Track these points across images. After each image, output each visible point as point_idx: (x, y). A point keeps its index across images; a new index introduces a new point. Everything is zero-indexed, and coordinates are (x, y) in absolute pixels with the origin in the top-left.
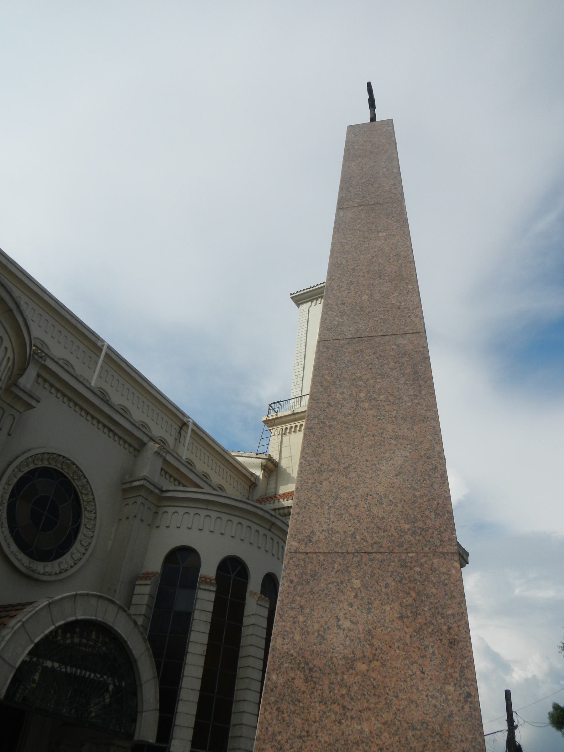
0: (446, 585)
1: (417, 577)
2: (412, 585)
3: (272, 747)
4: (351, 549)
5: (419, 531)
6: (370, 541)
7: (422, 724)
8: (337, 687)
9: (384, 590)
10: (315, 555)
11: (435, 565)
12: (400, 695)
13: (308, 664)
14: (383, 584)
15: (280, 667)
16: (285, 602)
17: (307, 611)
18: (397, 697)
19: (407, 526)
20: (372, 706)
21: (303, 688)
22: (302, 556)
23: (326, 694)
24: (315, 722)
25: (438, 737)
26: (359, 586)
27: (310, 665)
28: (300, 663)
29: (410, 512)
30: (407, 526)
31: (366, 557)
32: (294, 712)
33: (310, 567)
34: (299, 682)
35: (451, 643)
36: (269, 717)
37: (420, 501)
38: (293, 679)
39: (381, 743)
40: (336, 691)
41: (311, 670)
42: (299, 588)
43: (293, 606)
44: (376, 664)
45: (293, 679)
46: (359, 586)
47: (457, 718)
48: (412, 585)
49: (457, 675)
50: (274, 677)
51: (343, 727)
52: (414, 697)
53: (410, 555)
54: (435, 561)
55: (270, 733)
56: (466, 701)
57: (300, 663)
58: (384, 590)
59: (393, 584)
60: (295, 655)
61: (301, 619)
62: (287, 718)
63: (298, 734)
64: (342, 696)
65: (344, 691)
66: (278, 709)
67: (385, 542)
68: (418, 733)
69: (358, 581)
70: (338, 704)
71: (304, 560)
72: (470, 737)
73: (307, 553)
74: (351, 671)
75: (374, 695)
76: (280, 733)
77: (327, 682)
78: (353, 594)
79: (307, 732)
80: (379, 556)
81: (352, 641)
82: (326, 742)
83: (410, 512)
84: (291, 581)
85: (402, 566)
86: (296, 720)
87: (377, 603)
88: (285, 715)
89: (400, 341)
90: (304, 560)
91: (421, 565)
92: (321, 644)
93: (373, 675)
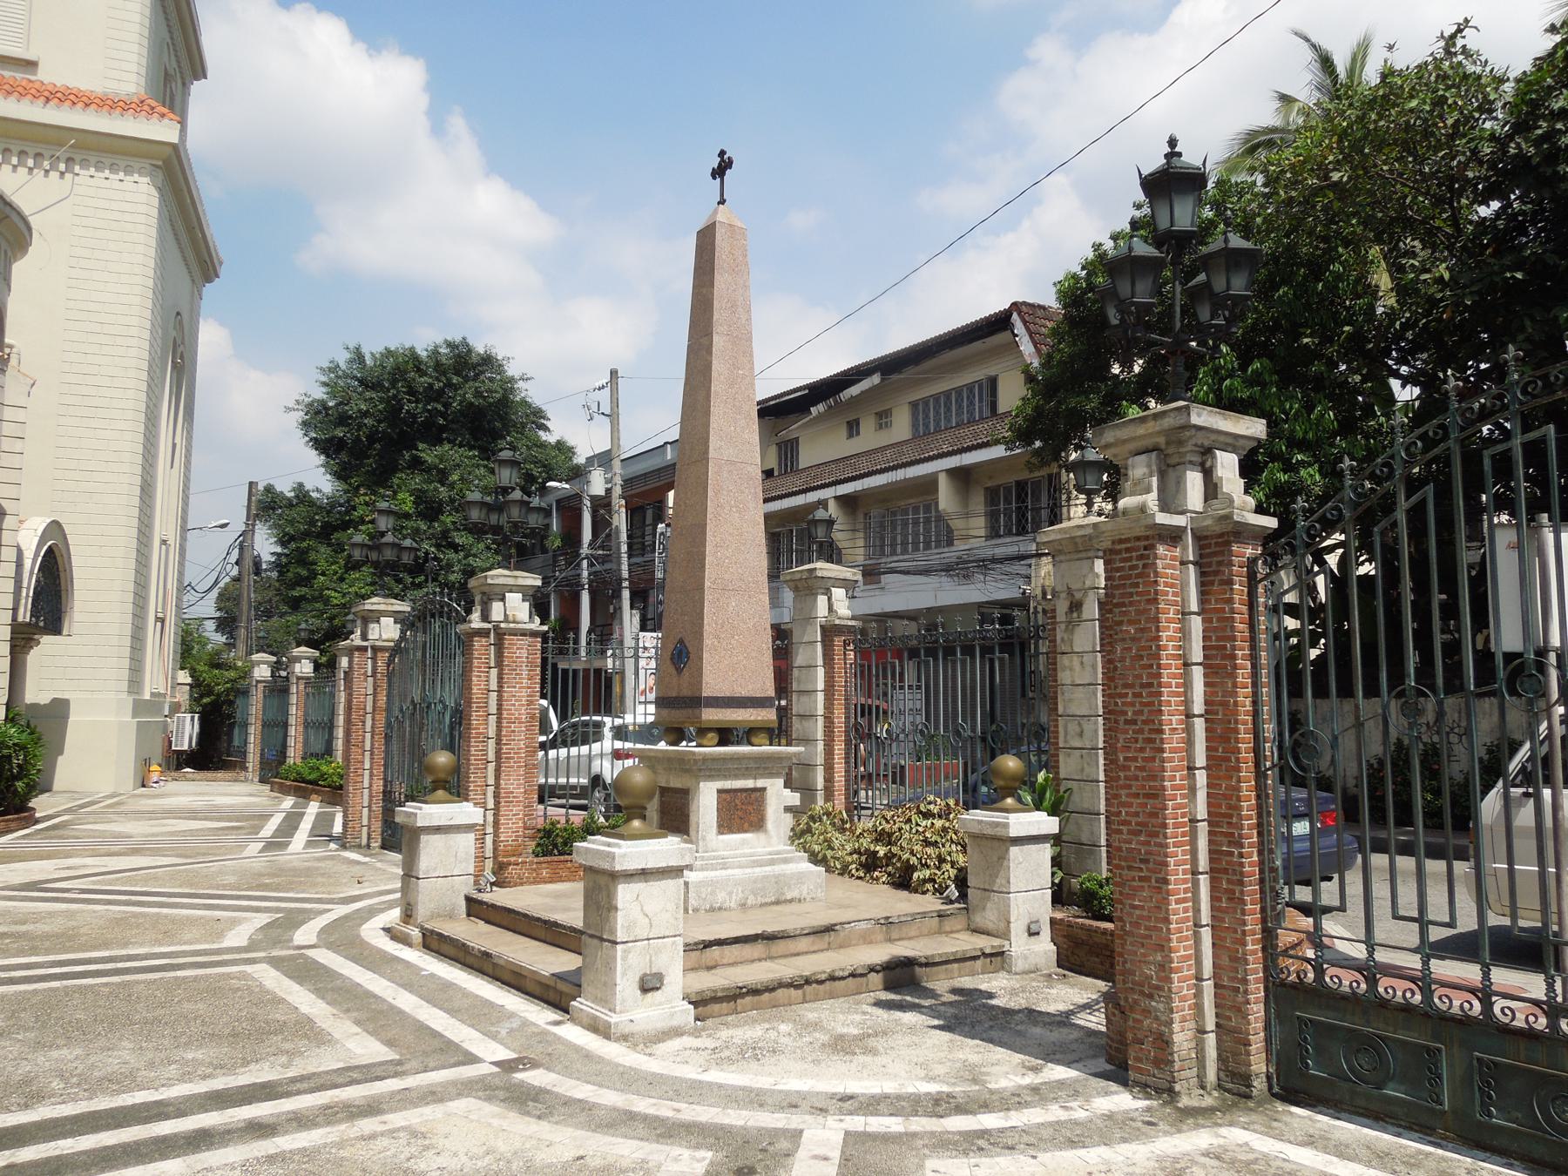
89: (749, 469)
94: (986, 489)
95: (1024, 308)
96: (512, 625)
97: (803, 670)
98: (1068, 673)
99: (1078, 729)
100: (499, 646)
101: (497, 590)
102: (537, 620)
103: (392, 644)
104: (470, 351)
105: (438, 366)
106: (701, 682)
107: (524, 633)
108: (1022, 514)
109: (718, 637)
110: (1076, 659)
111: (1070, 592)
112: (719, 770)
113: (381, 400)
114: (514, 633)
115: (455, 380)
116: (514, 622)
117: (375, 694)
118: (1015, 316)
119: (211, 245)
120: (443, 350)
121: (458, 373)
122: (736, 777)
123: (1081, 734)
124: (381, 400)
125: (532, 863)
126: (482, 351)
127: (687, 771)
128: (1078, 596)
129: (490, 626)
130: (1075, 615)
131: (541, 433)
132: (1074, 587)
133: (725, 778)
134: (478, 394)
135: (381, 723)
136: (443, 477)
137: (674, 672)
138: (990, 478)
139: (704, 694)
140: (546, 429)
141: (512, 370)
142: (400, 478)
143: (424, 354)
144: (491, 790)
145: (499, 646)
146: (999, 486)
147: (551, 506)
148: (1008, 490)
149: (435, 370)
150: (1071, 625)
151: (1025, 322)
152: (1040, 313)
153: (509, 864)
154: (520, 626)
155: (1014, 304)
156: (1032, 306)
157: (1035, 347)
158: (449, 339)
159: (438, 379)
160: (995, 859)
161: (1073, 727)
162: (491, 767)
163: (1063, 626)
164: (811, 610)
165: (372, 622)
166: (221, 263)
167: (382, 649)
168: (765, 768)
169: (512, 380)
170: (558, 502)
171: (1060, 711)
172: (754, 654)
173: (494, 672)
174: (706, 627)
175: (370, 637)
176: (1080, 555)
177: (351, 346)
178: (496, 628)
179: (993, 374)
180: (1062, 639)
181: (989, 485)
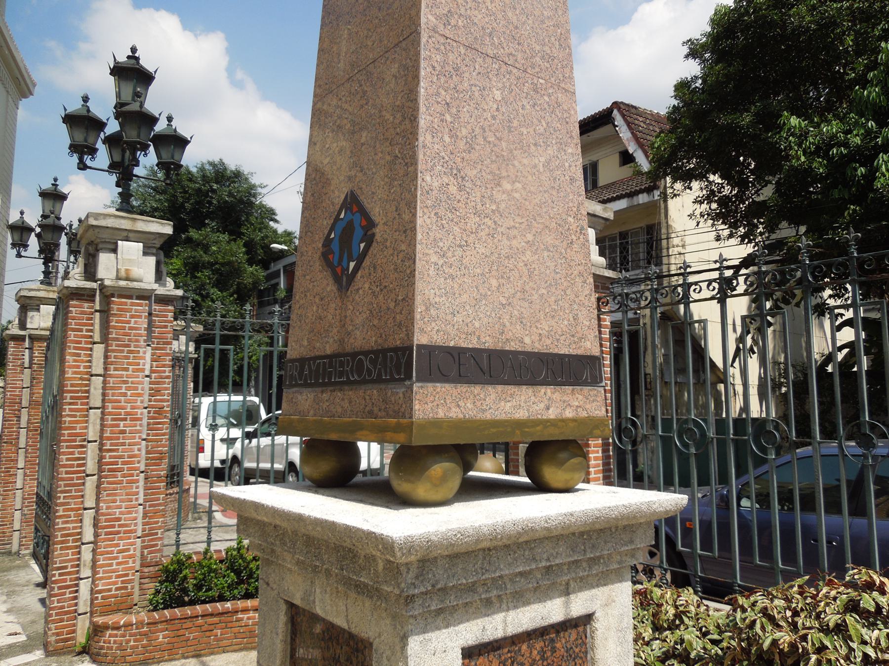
0: (567, 123)
1: (546, 106)
2: (542, 114)
3: (435, 253)
4: (490, 52)
5: (547, 57)
6: (507, 51)
7: (554, 247)
8: (488, 202)
9: (521, 110)
10: (455, 44)
11: (560, 99)
12: (538, 218)
13: (460, 172)
14: (520, 104)
15: (432, 169)
16: (431, 92)
17: (454, 110)
18: (535, 220)
19: (538, 48)
20: (517, 225)
21: (458, 197)
22: (442, 40)
23: (479, 206)
24: (472, 233)
25: (564, 259)
26: (500, 98)
27: (462, 173)
28: (451, 169)
29: (540, 32)
30: (538, 48)
31: (504, 67)
32: (452, 221)
33: (451, 56)
34: (453, 189)
35: (571, 179)
36: (428, 221)
37: (547, 23)
38: (448, 184)
39: (526, 260)
40: (488, 206)
41: (463, 178)
42: (443, 79)
43: (439, 100)
44: (518, 185)
45: (448, 184)
46: (500, 98)
47: (576, 246)
48: (542, 114)
49: (575, 209)
50: (428, 178)
51: (496, 241)
52: (548, 223)
53: (541, 81)
54: (560, 95)
55: (431, 238)
56: (581, 233)
57: (451, 169)
58: (521, 110)
59: (528, 107)
60: (447, 158)
61: (448, 118)
62: (446, 226)
63: (458, 243)
64: (493, 211)
65: (494, 207)
66: (436, 214)
67: (519, 56)
68: (551, 254)
69: (498, 93)
70: (490, 219)
71: (444, 44)
72: (584, 262)
73: (447, 38)
74: (499, 188)
75: (519, 215)
76: (441, 239)
77: (478, 194)
78: (495, 106)
79: (466, 242)
80: (515, 71)
81: (497, 157)
82: (483, 254)
83: (540, 32)
84: (434, 67)
85: (534, 90)
86: (455, 228)
87: (515, 123)
88: (444, 222)
90: (444, 44)
91: (549, 96)
92: (470, 152)
93: (517, 195)
95: (622, 106)
96: (123, 283)
100: (105, 312)
101: (105, 235)
102: (170, 283)
103: (48, 333)
104: (225, 169)
105: (204, 177)
106: (408, 301)
107: (144, 295)
109: (457, 174)
112: (471, 588)
113: (167, 200)
114: (127, 294)
115: (215, 186)
116: (127, 279)
117: (31, 387)
118: (615, 112)
119: (21, 65)
120: (207, 167)
121: (217, 183)
122: (519, 599)
124: (167, 200)
125: (140, 624)
126: (233, 168)
127: (361, 589)
129: (94, 285)
131: (271, 223)
133: (488, 607)
134: (230, 194)
135: (36, 420)
136: (206, 248)
137: (331, 287)
139: (420, 339)
140: (276, 221)
141: (254, 180)
142: (177, 250)
143: (194, 170)
144: (89, 516)
145: (105, 312)
146: (606, 237)
147: (279, 270)
149: (203, 180)
151: (623, 116)
152: (633, 110)
153: (106, 627)
154: (135, 285)
155: (616, 104)
156: (628, 105)
157: (632, 133)
158: (211, 160)
159: (204, 185)
162: (91, 482)
165: (32, 310)
166: (34, 85)
167: (40, 338)
168: (594, 561)
169: (253, 187)
170: (285, 267)
172: (549, 239)
173: (99, 349)
174: (424, 138)
175: (29, 326)
177: (148, 166)
178: (102, 287)
179: (595, 159)
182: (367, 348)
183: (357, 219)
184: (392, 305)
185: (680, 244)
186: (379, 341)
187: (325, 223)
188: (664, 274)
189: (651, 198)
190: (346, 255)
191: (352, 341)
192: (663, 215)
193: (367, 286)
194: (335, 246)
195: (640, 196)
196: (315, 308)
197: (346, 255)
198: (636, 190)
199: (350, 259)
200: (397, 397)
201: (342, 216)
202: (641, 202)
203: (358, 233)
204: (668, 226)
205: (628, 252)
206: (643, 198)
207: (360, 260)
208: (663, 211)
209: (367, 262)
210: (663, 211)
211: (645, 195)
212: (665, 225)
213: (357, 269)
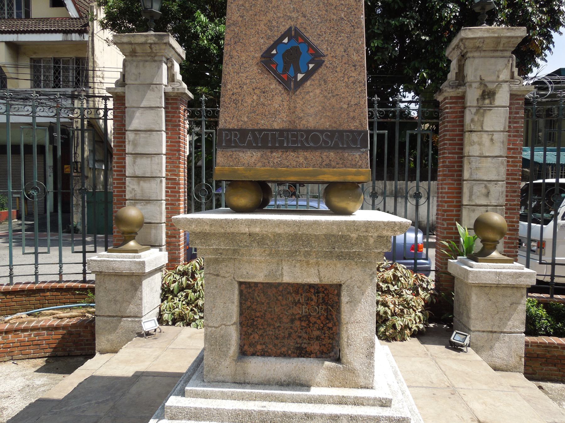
94: (31, 59)
97: (142, 135)
98: (476, 147)
99: (484, 191)
108: (57, 78)
110: (485, 136)
111: (482, 82)
123: (487, 195)
128: (491, 86)
130: (487, 101)
132: (487, 79)
138: (35, 53)
146: (41, 58)
148: (47, 61)
150: (481, 110)
160: (507, 304)
161: (479, 189)
163: (474, 110)
164: (153, 76)
171: (466, 175)
176: (499, 54)
180: (472, 121)
181: (34, 56)
182: (321, 128)
183: (303, 48)
184: (345, 106)
185: (101, 76)
186: (334, 125)
187: (262, 41)
188: (96, 95)
189: (82, 39)
190: (292, 69)
191: (304, 122)
192: (90, 53)
193: (318, 91)
194: (279, 61)
195: (73, 35)
196: (255, 97)
197: (292, 69)
198: (70, 30)
199: (298, 71)
200: (354, 157)
201: (286, 41)
202: (74, 39)
203: (305, 56)
204: (94, 62)
205: (59, 73)
206: (75, 37)
207: (309, 74)
208: (90, 50)
209: (316, 76)
210: (90, 50)
211: (77, 35)
212: (92, 60)
213: (304, 80)
